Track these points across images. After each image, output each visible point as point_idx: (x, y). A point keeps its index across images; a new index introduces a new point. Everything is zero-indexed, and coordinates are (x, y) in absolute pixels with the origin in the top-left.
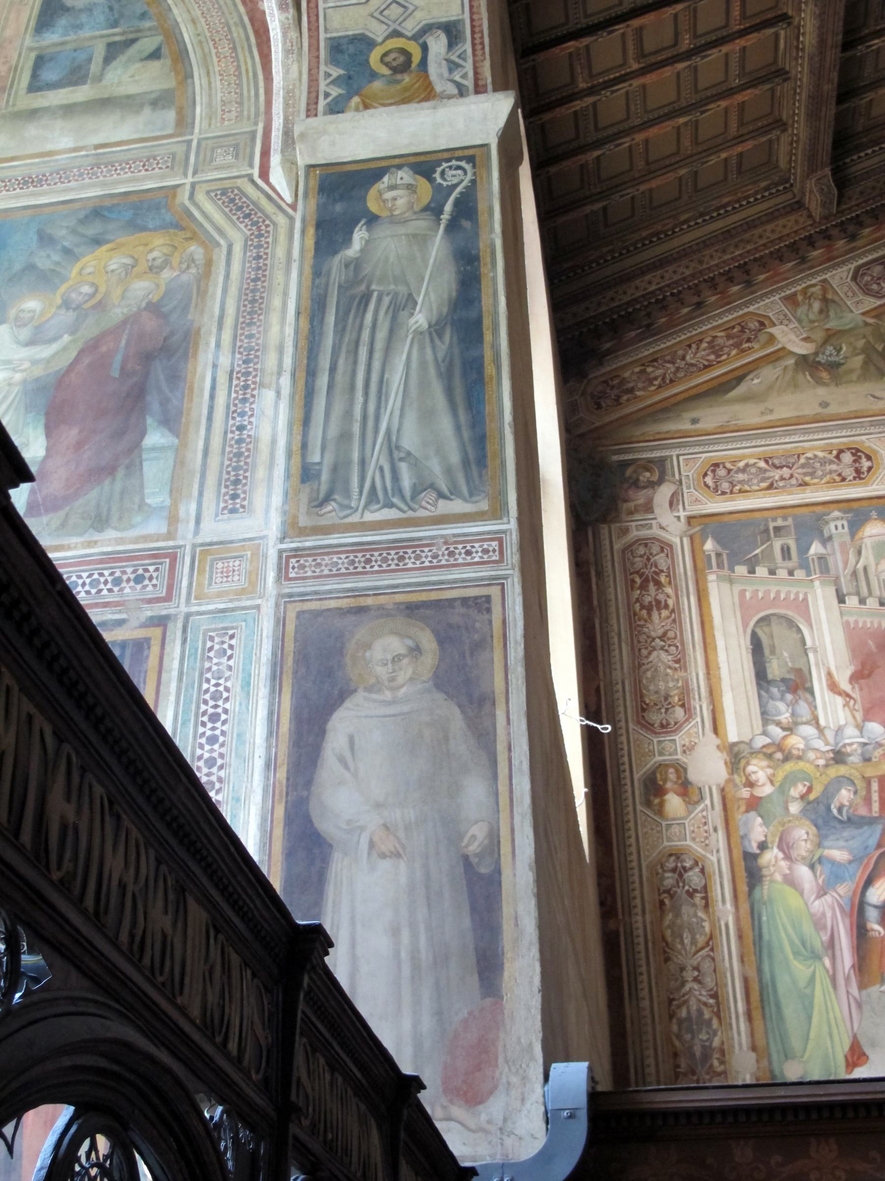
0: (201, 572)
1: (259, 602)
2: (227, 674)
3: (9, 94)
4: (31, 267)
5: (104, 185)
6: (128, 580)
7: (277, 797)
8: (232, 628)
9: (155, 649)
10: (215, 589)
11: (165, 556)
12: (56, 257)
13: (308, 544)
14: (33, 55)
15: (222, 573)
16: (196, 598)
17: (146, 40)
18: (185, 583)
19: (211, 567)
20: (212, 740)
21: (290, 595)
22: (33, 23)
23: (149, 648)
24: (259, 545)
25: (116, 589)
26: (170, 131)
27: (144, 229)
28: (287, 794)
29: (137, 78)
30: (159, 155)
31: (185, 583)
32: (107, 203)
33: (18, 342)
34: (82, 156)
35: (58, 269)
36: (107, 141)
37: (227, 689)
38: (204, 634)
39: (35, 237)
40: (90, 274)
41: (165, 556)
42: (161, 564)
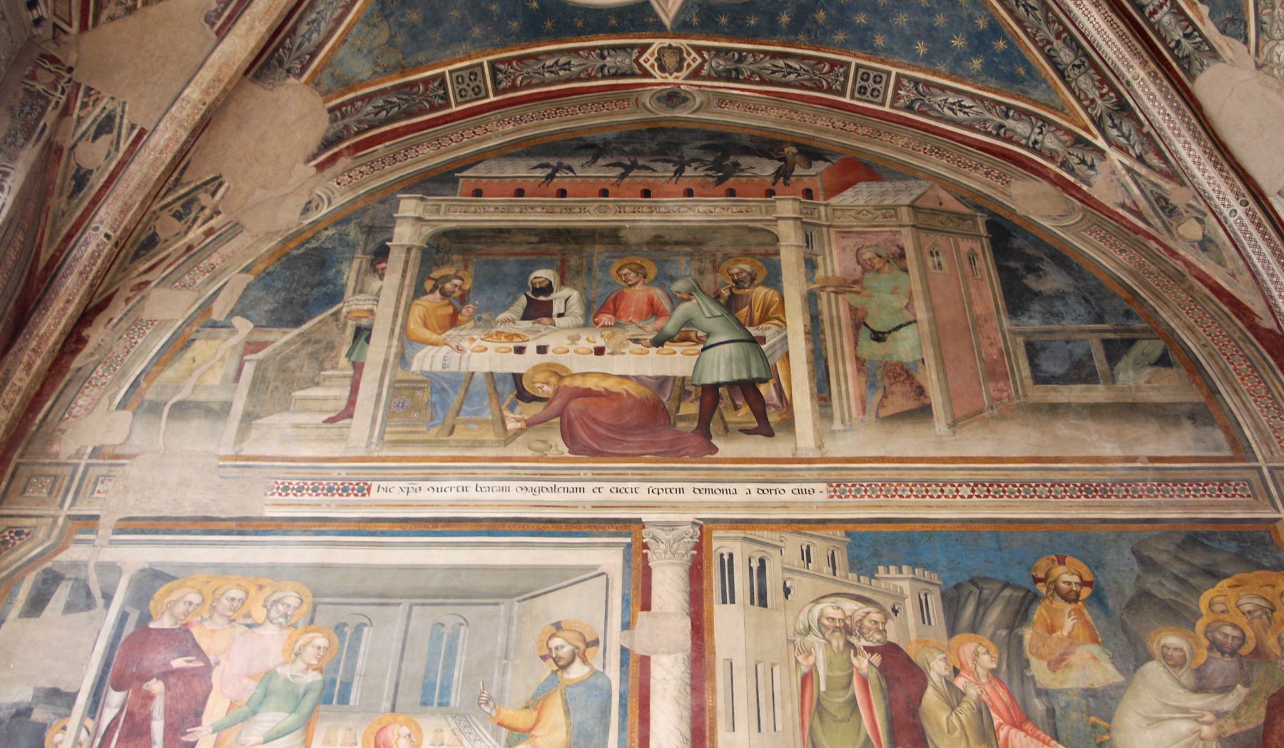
3: (1015, 382)
4: (1144, 596)
5: (1184, 506)
12: (1174, 588)
14: (1020, 340)
17: (1145, 343)
22: (1001, 303)
26: (1227, 453)
27: (1260, 567)
29: (1155, 385)
30: (1232, 480)
32: (1199, 528)
33: (1184, 687)
34: (1141, 469)
35: (1180, 600)
36: (1158, 454)
39: (1133, 559)
40: (1222, 612)
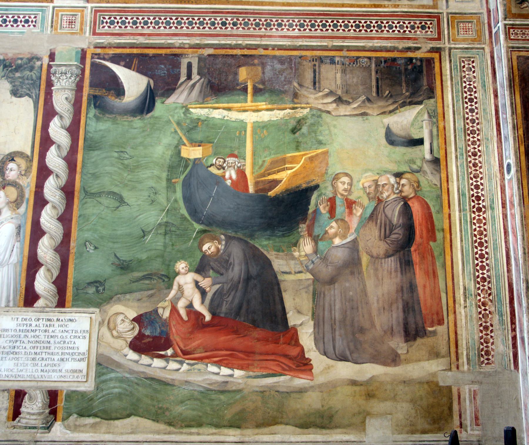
0: (453, 28)
1: (483, 46)
2: (474, 80)
6: (418, 27)
7: (520, 143)
8: (473, 58)
9: (437, 64)
10: (461, 37)
11: (435, 17)
13: (517, 23)
15: (463, 29)
16: (453, 41)
18: (446, 32)
19: (457, 25)
20: (472, 111)
21: (513, 48)
23: (434, 63)
24: (480, 17)
25: (413, 31)
28: (524, 141)
31: (446, 32)
37: (475, 87)
38: (460, 59)
41: (435, 17)
42: (433, 21)
